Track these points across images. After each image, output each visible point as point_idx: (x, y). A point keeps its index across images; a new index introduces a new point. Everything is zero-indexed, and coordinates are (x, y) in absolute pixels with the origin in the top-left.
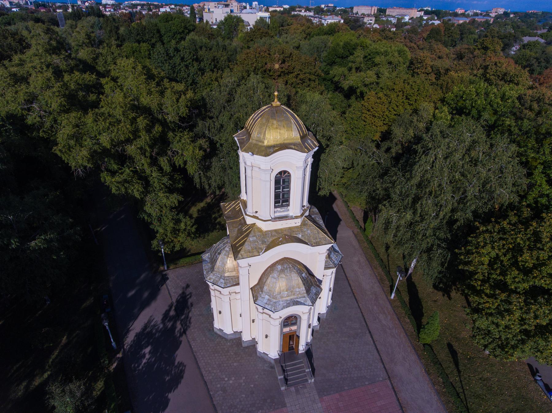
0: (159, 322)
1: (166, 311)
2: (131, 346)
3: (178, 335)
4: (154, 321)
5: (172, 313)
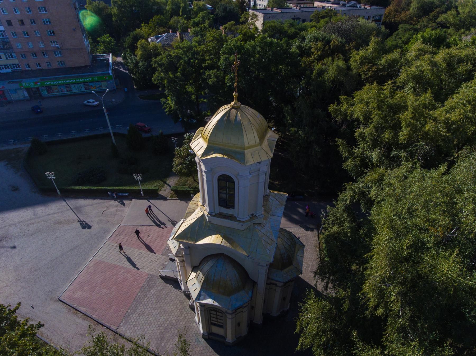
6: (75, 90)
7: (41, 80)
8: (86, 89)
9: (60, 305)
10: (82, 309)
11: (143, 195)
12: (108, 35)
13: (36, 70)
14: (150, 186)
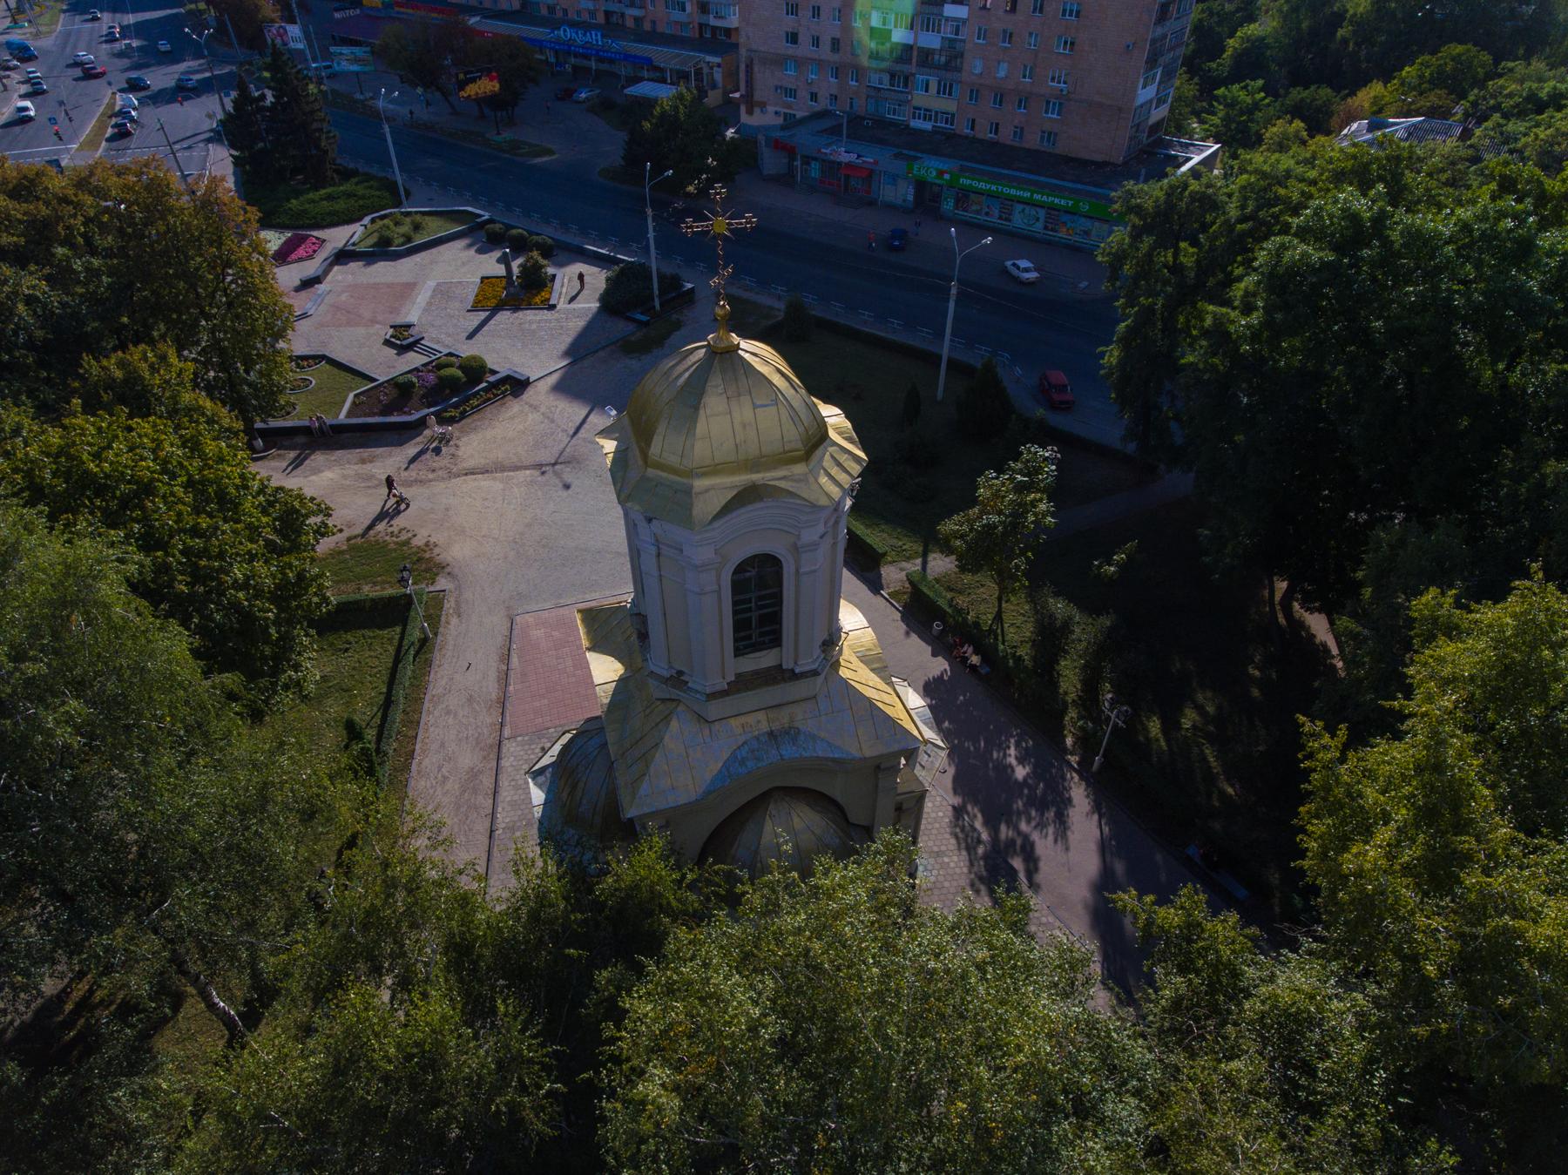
0: (1035, 836)
1: (1037, 869)
2: (1064, 779)
3: (969, 808)
4: (1051, 838)
5: (1017, 863)
6: (1019, 220)
10: (515, 660)
13: (981, 141)
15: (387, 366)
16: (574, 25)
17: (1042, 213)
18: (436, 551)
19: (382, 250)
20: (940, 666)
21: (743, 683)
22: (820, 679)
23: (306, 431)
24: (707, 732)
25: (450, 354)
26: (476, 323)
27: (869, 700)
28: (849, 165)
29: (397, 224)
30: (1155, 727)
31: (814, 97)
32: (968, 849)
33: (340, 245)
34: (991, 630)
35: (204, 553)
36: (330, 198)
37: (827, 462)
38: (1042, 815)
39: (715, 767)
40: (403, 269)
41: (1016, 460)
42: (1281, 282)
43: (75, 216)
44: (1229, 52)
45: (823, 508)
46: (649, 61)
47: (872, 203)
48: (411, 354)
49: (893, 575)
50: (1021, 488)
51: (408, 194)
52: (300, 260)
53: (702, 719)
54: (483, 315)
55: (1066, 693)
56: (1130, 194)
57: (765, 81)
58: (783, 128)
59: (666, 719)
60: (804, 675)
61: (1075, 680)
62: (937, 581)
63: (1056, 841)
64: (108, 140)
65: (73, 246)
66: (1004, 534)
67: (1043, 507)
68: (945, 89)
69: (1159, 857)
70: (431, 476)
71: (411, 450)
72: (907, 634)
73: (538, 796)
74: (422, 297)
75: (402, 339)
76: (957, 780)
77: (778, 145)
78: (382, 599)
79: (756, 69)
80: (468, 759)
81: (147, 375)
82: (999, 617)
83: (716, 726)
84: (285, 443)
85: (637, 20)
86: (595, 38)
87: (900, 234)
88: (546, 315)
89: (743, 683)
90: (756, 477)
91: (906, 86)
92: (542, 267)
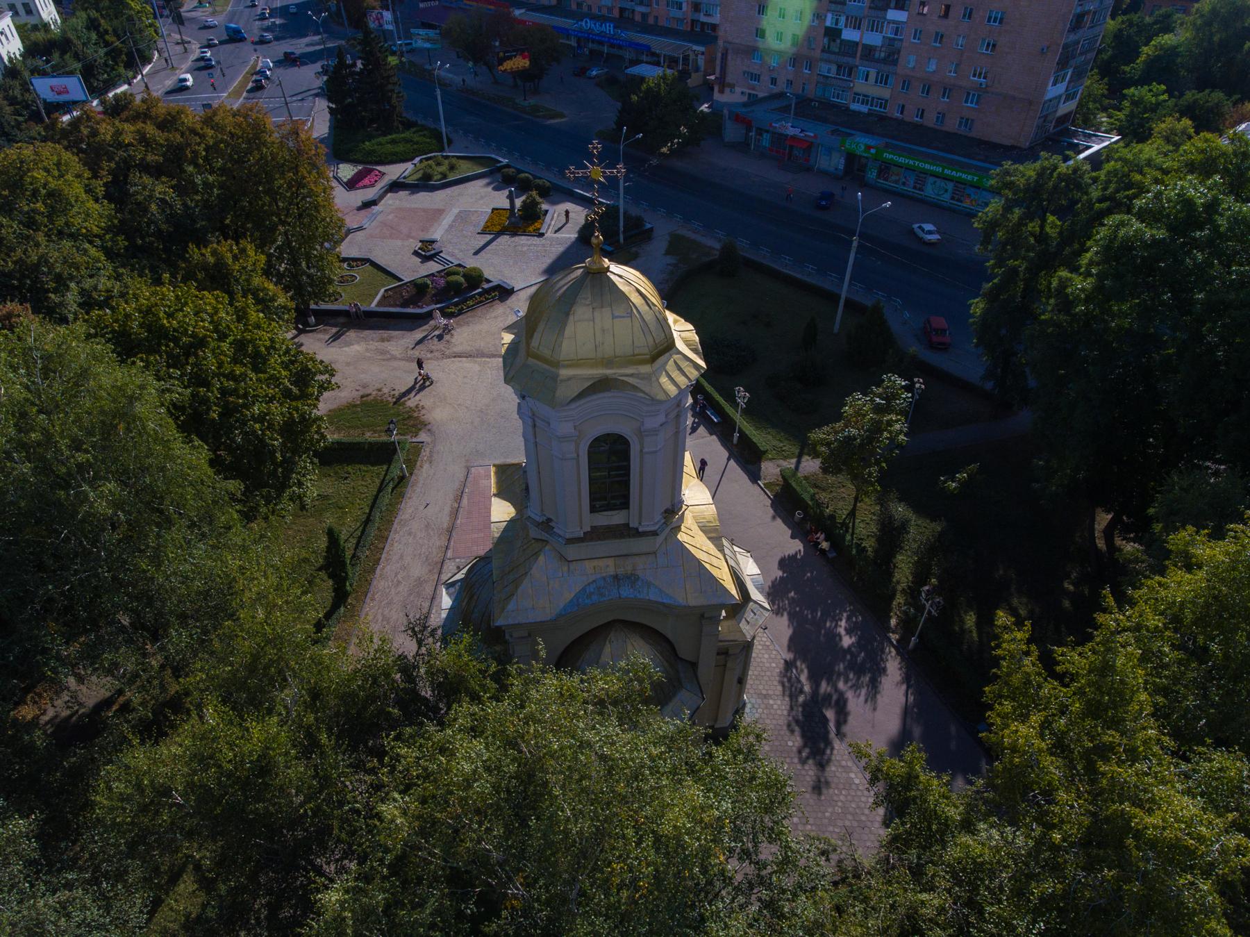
0: (850, 695)
1: (845, 722)
2: (883, 652)
3: (798, 663)
4: (862, 698)
5: (830, 714)
6: (929, 191)
7: (887, 146)
8: (953, 198)
9: (461, 476)
10: (465, 501)
11: (735, 440)
12: (1163, 87)
14: (760, 437)
15: (412, 270)
16: (594, 18)
17: (950, 186)
18: (423, 412)
19: (424, 184)
20: (796, 546)
21: (596, 534)
22: (660, 539)
23: (346, 313)
24: (565, 569)
25: (459, 265)
26: (482, 243)
27: (698, 561)
28: (793, 138)
29: (439, 164)
30: (970, 620)
31: (774, 81)
32: (791, 696)
33: (394, 178)
34: (844, 524)
35: (234, 392)
36: (393, 142)
37: (670, 366)
38: (859, 679)
39: (568, 596)
40: (438, 198)
41: (878, 386)
42: (1117, 253)
43: (199, 144)
44: (1143, 58)
45: (660, 402)
46: (648, 48)
47: (809, 170)
48: (432, 263)
49: (770, 469)
50: (878, 409)
51: (450, 142)
52: (365, 187)
53: (562, 558)
54: (489, 237)
55: (898, 582)
56: (1007, 173)
57: (736, 67)
58: (745, 105)
59: (536, 554)
60: (645, 534)
61: (907, 572)
62: (806, 478)
63: (866, 701)
64: (248, 91)
65: (196, 165)
66: (861, 445)
67: (898, 426)
68: (883, 80)
69: (953, 729)
70: (429, 355)
71: (418, 334)
72: (774, 518)
73: (446, 601)
74: (447, 220)
75: (427, 251)
76: (792, 640)
77: (737, 118)
78: (377, 443)
79: (729, 58)
80: (418, 570)
81: (230, 261)
82: (852, 514)
83: (573, 566)
84: (332, 321)
85: (644, 16)
86: (609, 28)
87: (828, 196)
88: (536, 240)
89: (596, 534)
90: (608, 372)
91: (850, 75)
92: (538, 203)
